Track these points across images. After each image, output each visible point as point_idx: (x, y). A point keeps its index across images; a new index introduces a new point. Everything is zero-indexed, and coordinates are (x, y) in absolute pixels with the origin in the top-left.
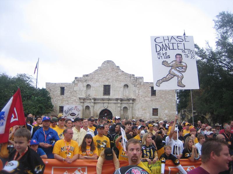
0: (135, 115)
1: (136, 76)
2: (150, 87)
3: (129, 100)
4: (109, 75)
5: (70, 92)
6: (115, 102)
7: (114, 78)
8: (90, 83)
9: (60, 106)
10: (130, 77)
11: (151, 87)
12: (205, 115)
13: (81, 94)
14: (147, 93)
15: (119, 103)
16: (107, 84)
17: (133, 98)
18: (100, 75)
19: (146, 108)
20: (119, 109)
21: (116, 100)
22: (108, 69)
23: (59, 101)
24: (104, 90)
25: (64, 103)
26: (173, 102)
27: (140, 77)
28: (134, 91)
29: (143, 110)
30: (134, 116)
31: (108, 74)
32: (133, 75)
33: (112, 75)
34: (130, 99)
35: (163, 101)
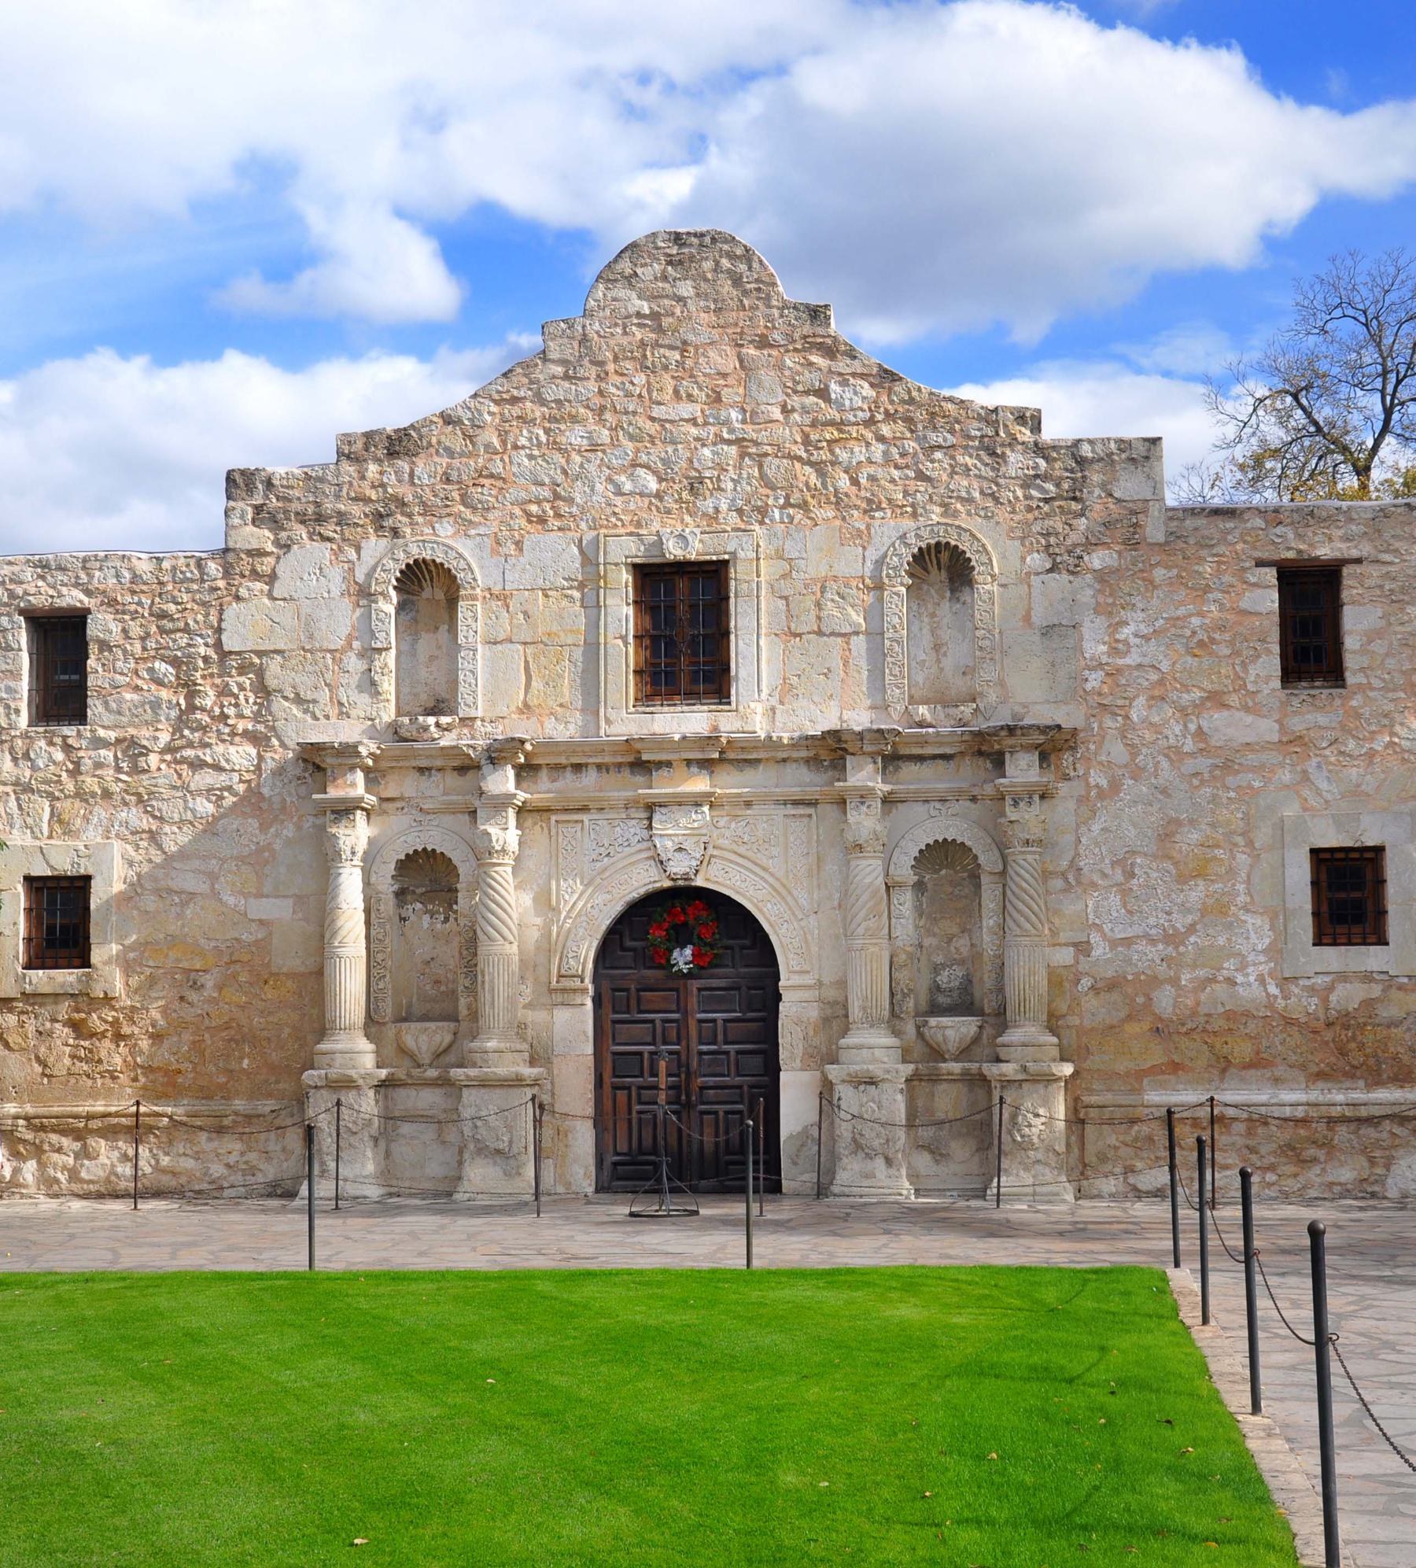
0: (1082, 948)
1: (1052, 431)
2: (1260, 563)
6: (801, 780)
9: (29, 880)
10: (992, 451)
11: (1270, 575)
15: (864, 796)
18: (575, 436)
19: (1219, 852)
20: (869, 871)
21: (814, 762)
27: (1124, 444)
28: (1048, 631)
29: (1182, 879)
30: (1064, 956)
31: (686, 410)
34: (1011, 730)
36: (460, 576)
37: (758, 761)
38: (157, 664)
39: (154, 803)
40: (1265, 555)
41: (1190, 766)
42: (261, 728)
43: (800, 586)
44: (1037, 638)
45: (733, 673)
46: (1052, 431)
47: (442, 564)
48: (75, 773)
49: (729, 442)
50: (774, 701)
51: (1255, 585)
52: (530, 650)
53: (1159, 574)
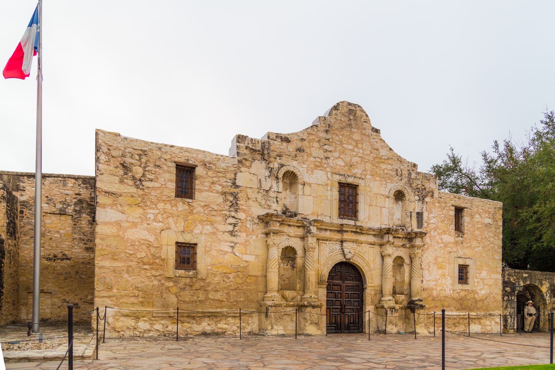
1: (419, 170)
2: (452, 206)
3: (410, 237)
4: (355, 154)
5: (219, 188)
6: (371, 239)
7: (368, 166)
8: (293, 165)
9: (177, 243)
11: (453, 208)
12: (542, 285)
13: (263, 202)
14: (446, 222)
16: (350, 180)
17: (416, 230)
22: (351, 132)
23: (171, 220)
24: (340, 201)
25: (197, 231)
26: (495, 251)
28: (418, 213)
31: (350, 147)
32: (415, 166)
33: (363, 153)
35: (478, 247)
36: (299, 177)
37: (364, 233)
38: (217, 186)
39: (216, 225)
40: (454, 204)
41: (439, 246)
42: (246, 208)
43: (373, 194)
44: (416, 214)
45: (359, 212)
46: (419, 170)
47: (295, 173)
48: (191, 213)
49: (360, 157)
50: (367, 220)
51: (451, 210)
52: (315, 199)
53: (437, 204)
